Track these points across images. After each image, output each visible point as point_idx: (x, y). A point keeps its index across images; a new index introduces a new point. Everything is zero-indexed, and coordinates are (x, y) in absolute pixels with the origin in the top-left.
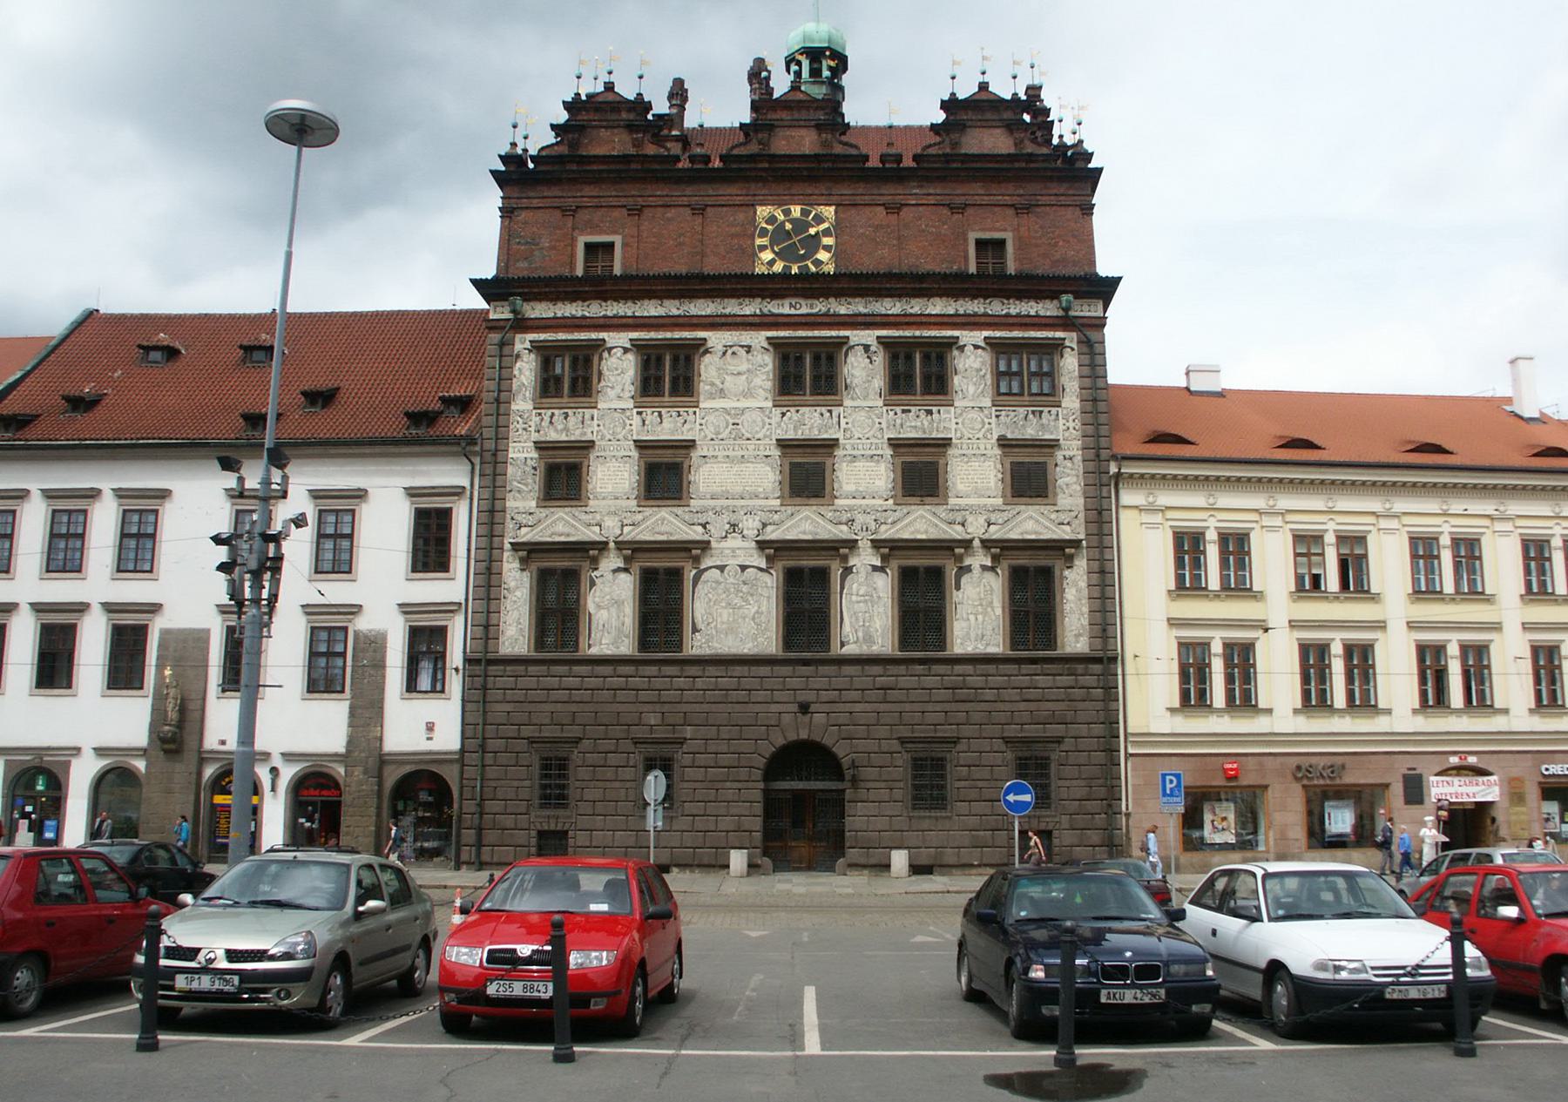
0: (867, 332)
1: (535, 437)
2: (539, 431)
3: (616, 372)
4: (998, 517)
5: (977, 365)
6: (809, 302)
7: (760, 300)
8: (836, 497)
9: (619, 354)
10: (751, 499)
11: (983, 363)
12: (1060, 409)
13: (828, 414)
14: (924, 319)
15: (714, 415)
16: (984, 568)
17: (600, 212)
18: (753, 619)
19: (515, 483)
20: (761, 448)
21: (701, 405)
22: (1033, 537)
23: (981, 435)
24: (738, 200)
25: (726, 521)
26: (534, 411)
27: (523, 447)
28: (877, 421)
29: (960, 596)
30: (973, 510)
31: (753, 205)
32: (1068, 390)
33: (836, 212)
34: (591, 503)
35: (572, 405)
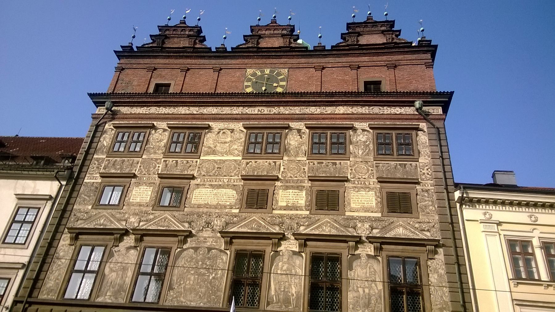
0: (300, 123)
1: (102, 171)
2: (105, 169)
3: (156, 141)
4: (380, 225)
5: (363, 140)
6: (269, 109)
7: (242, 108)
8: (273, 209)
9: (160, 132)
10: (221, 208)
11: (368, 139)
12: (417, 163)
13: (274, 164)
14: (333, 116)
15: (207, 163)
16: (369, 256)
17: (166, 71)
18: (210, 285)
19: (83, 196)
20: (232, 181)
21: (202, 158)
22: (404, 237)
23: (367, 177)
24: (237, 66)
25: (204, 221)
26: (106, 159)
27: (94, 177)
28: (303, 167)
29: (353, 274)
30: (363, 220)
31: (245, 68)
32: (423, 153)
33: (288, 71)
34: (124, 207)
35: (128, 156)
